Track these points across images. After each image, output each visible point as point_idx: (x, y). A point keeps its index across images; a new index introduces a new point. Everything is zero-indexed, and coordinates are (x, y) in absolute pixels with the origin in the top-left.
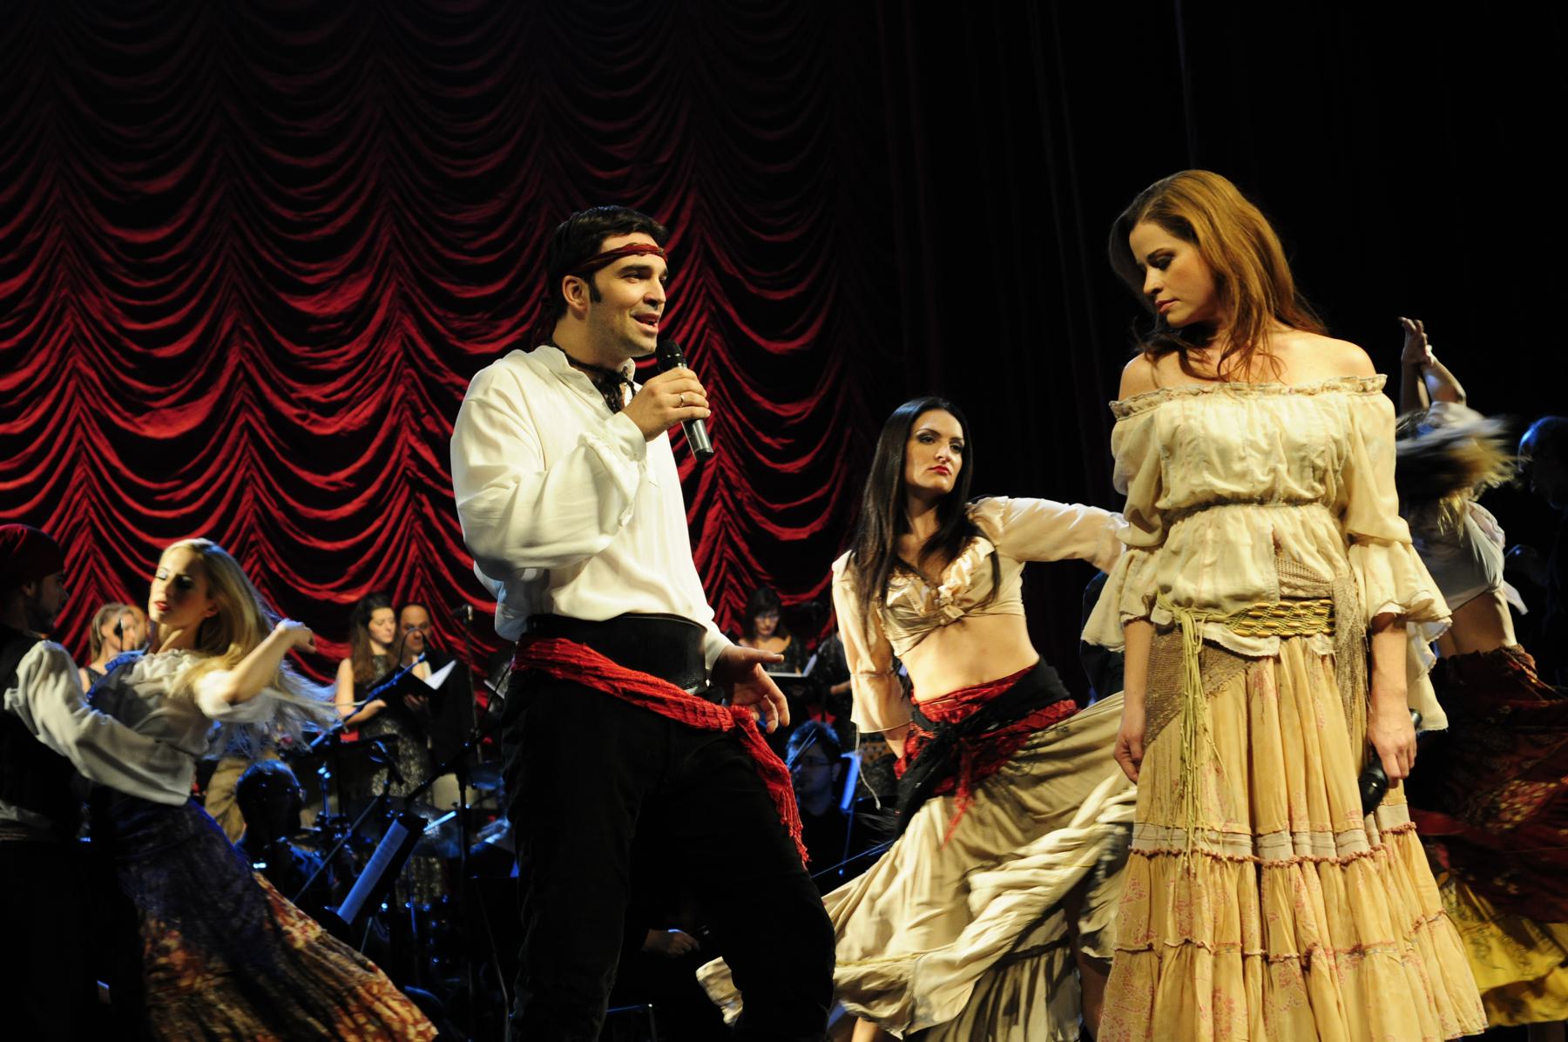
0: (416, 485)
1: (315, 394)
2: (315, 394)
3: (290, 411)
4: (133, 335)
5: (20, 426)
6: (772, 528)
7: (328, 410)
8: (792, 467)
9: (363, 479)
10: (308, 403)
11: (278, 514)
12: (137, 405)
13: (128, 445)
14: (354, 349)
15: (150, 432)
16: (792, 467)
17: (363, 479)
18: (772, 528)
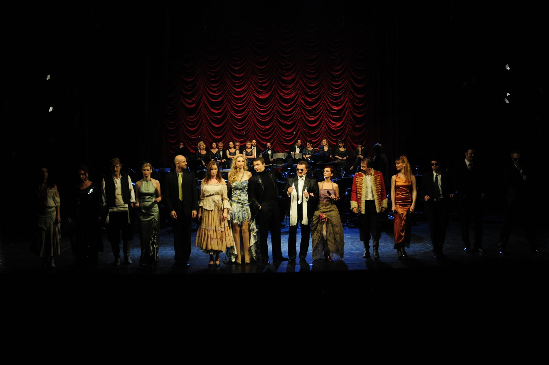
0: (301, 106)
1: (286, 92)
2: (286, 92)
3: (282, 95)
4: (259, 83)
5: (242, 96)
6: (356, 115)
7: (288, 94)
8: (360, 105)
9: (292, 105)
10: (285, 94)
11: (279, 110)
12: (259, 93)
13: (257, 99)
14: (292, 85)
15: (261, 97)
16: (360, 105)
17: (292, 105)
18: (356, 115)
